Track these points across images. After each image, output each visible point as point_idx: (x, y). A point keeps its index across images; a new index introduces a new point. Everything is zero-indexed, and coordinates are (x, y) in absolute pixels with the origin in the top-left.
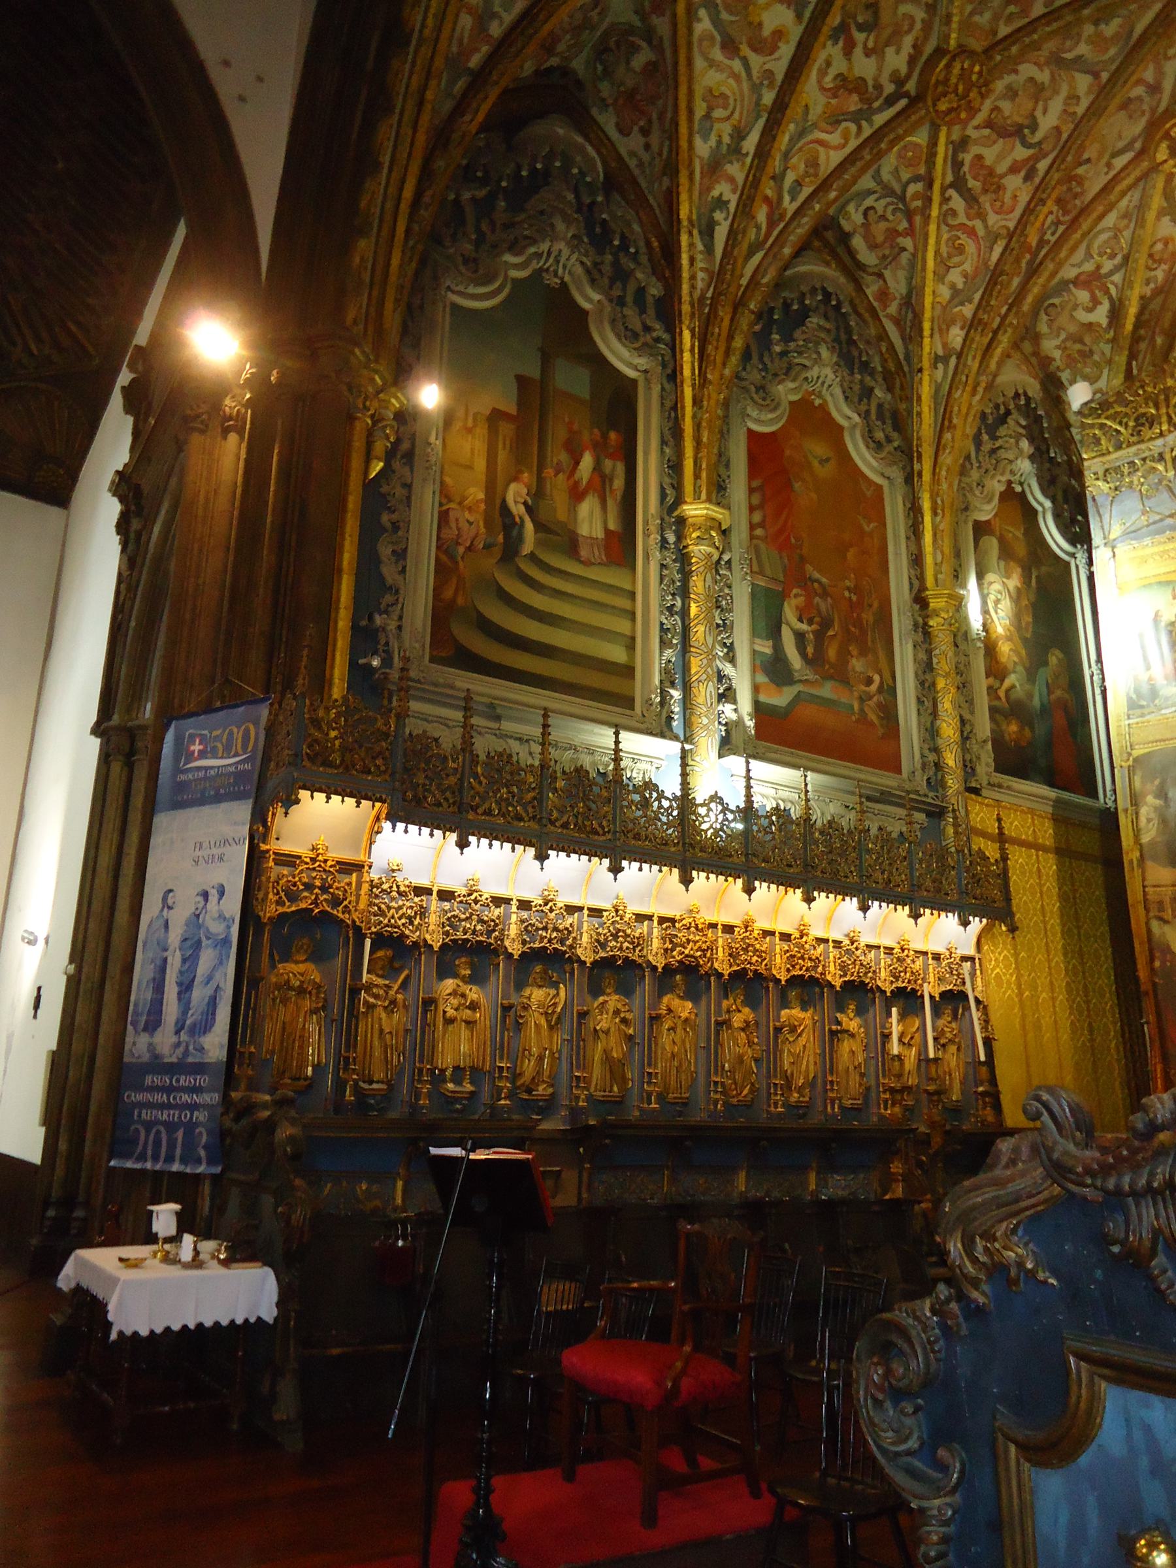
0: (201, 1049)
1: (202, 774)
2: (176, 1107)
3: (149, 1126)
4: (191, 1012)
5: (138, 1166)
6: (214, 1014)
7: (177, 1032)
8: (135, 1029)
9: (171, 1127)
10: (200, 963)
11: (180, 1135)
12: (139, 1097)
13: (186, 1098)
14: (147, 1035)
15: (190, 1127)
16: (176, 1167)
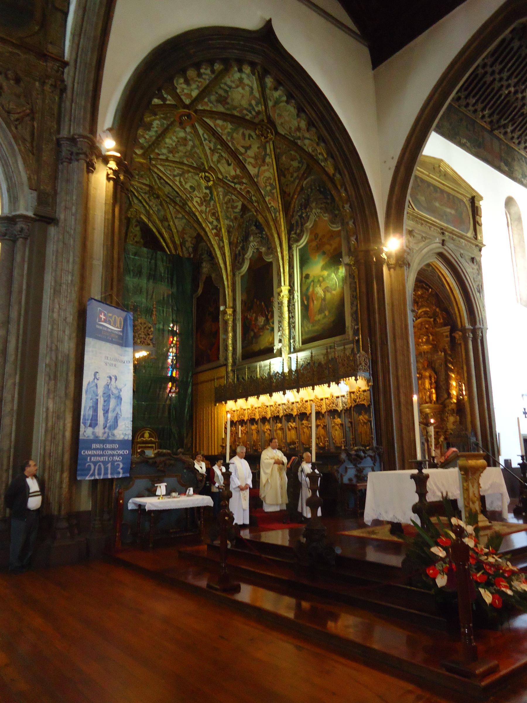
0: (114, 435)
1: (106, 329)
2: (106, 455)
3: (95, 463)
4: (108, 421)
5: (93, 478)
6: (117, 422)
7: (104, 428)
8: (85, 425)
9: (105, 463)
10: (111, 403)
11: (109, 465)
12: (90, 452)
13: (110, 452)
14: (91, 428)
15: (113, 462)
16: (109, 477)
